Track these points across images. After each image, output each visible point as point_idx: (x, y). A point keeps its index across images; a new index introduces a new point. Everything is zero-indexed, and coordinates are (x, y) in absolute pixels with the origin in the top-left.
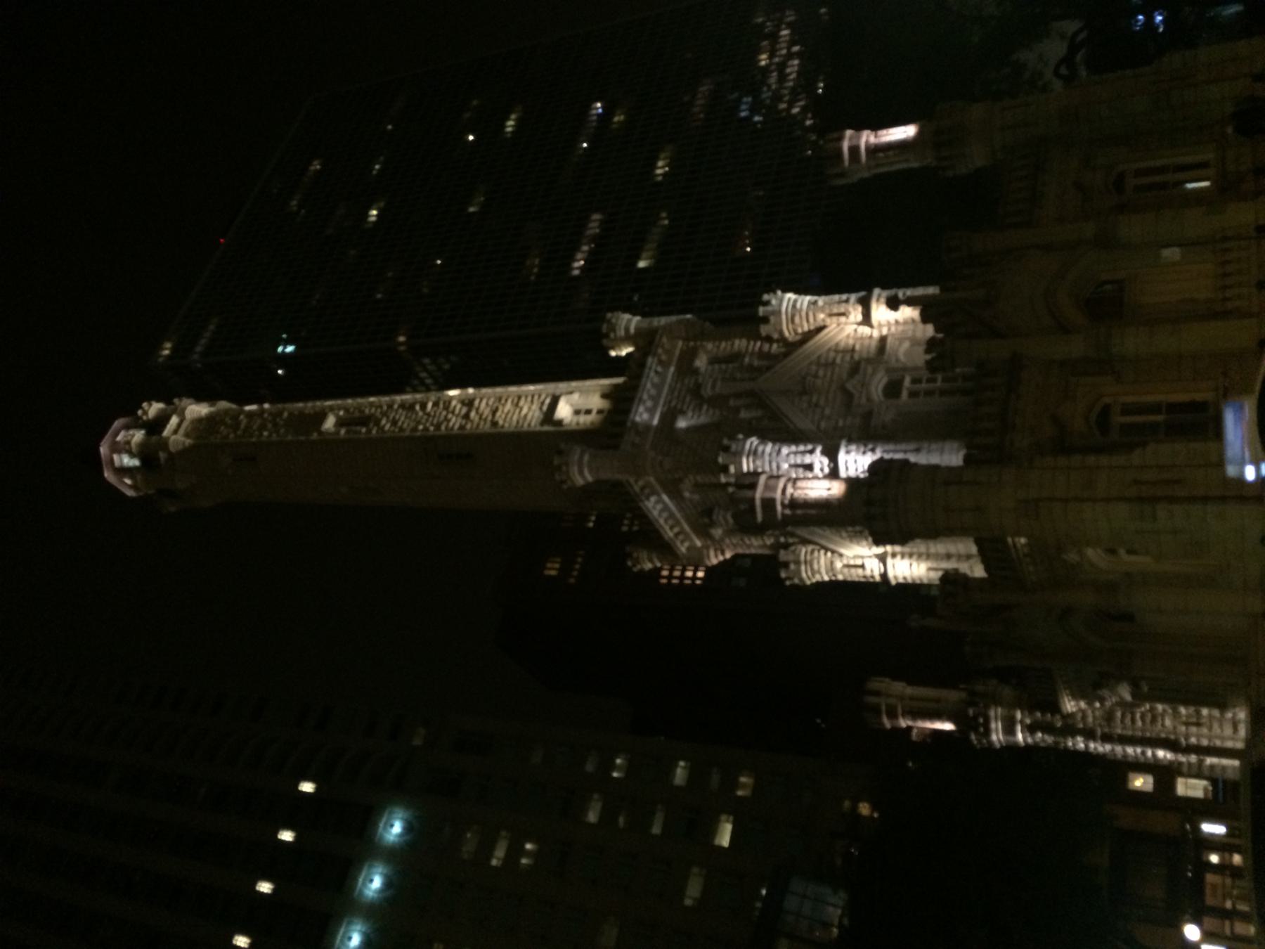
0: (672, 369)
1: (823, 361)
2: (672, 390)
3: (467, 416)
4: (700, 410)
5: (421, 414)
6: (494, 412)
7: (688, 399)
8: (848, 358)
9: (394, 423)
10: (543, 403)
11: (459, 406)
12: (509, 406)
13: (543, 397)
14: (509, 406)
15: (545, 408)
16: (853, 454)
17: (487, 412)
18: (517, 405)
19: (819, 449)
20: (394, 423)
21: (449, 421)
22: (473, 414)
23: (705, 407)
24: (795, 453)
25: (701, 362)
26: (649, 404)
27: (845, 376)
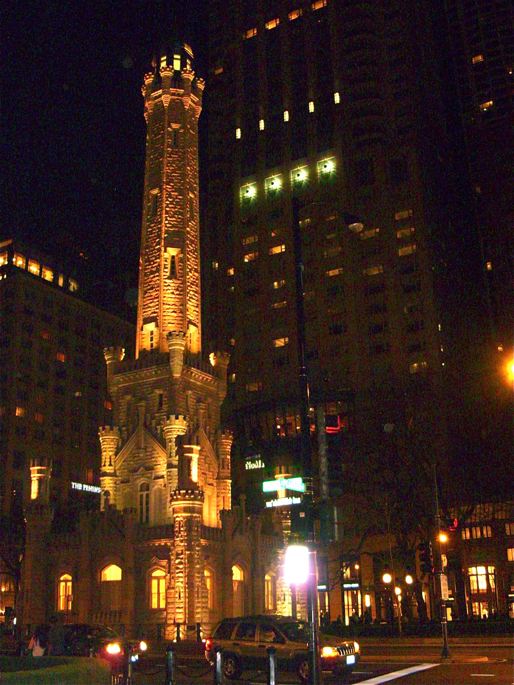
0: (155, 379)
1: (153, 452)
6: (152, 288)
8: (155, 464)
10: (155, 313)
11: (156, 265)
13: (157, 311)
22: (152, 276)
25: (158, 392)
27: (148, 465)
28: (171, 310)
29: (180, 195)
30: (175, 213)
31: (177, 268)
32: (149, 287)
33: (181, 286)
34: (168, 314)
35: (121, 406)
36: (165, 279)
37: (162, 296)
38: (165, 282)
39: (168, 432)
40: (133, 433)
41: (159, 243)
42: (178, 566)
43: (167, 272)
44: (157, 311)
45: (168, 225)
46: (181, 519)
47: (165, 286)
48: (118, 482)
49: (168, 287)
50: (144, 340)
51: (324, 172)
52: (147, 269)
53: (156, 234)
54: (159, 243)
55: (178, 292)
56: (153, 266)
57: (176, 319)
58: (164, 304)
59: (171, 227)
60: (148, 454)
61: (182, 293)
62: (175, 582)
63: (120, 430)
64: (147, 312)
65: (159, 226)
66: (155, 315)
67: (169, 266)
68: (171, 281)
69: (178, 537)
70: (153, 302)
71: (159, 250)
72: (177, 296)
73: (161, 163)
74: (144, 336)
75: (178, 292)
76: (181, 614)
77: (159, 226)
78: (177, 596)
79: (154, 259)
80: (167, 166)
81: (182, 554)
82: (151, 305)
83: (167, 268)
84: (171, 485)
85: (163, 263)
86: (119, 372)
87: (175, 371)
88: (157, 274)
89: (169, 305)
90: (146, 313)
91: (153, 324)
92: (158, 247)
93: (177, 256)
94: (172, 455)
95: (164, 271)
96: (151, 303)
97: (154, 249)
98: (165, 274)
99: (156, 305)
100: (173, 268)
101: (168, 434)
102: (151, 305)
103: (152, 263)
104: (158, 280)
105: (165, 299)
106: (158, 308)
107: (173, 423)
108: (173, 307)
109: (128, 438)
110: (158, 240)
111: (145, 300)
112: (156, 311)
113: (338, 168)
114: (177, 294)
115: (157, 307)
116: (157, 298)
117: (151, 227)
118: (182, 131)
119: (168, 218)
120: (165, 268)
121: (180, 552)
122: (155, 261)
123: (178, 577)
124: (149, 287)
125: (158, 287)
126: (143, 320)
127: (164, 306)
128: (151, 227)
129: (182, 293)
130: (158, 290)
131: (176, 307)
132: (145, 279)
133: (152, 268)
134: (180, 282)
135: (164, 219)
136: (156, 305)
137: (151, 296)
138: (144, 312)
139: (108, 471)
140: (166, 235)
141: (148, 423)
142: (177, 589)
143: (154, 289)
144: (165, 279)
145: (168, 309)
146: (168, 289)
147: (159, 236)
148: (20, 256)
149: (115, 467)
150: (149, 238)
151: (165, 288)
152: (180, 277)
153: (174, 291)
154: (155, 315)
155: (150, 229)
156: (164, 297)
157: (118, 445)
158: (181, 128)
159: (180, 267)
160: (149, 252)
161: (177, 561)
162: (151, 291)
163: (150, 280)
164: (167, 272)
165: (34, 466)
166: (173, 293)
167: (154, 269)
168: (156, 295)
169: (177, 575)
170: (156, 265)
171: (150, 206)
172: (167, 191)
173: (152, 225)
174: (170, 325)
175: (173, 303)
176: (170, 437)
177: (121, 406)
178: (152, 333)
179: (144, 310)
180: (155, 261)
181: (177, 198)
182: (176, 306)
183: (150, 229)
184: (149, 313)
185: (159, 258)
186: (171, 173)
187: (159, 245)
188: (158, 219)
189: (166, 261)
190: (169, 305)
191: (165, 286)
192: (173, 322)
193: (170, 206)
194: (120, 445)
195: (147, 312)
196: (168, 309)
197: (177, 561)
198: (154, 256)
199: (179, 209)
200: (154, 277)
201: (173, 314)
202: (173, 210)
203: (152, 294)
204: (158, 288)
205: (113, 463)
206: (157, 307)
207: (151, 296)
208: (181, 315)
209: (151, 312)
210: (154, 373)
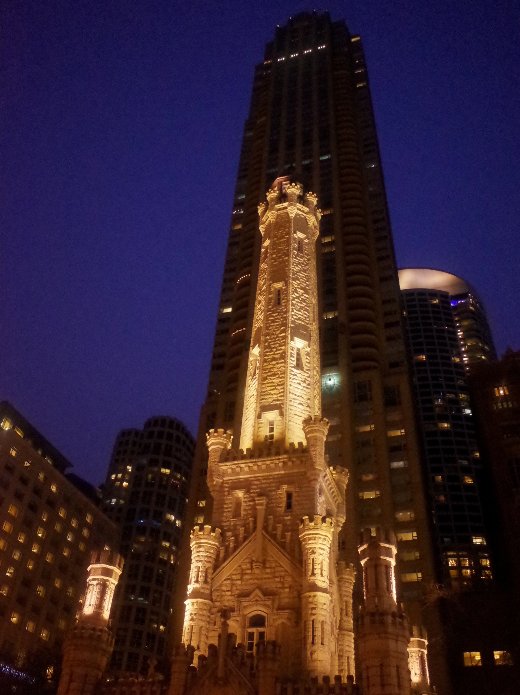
0: (283, 472)
2: (266, 478)
3: (274, 359)
4: (250, 501)
6: (274, 375)
7: (258, 490)
9: (273, 321)
10: (278, 400)
11: (280, 352)
12: (277, 381)
13: (282, 398)
14: (277, 381)
15: (274, 403)
16: (192, 608)
17: (275, 370)
18: (278, 385)
19: (198, 585)
20: (273, 321)
21: (271, 351)
22: (274, 362)
23: (251, 503)
24: (198, 572)
26: (264, 467)
28: (299, 402)
29: (305, 294)
30: (301, 308)
31: (303, 361)
32: (270, 374)
33: (309, 379)
34: (295, 405)
35: (226, 504)
36: (292, 367)
37: (289, 384)
38: (292, 371)
39: (310, 539)
40: (244, 541)
41: (284, 331)
43: (294, 361)
44: (282, 398)
45: (294, 317)
47: (292, 374)
48: (214, 610)
49: (295, 377)
50: (260, 429)
51: (329, 384)
52: (266, 356)
53: (280, 323)
54: (284, 331)
55: (305, 385)
56: (276, 353)
57: (303, 412)
58: (290, 392)
59: (298, 320)
60: (268, 571)
61: (309, 387)
63: (222, 534)
64: (266, 399)
65: (285, 315)
66: (278, 402)
67: (295, 356)
68: (298, 371)
70: (276, 389)
71: (285, 337)
72: (304, 389)
73: (288, 261)
74: (260, 425)
75: (305, 385)
77: (285, 315)
80: (293, 265)
82: (272, 392)
83: (293, 357)
84: (314, 617)
85: (290, 351)
86: (226, 460)
87: (318, 463)
88: (282, 361)
89: (296, 395)
90: (264, 401)
91: (277, 412)
92: (283, 334)
93: (303, 348)
94: (316, 572)
95: (291, 359)
96: (273, 390)
97: (278, 337)
98: (292, 362)
99: (280, 393)
100: (299, 360)
101: (310, 542)
102: (272, 392)
103: (275, 350)
104: (284, 367)
105: (291, 388)
106: (283, 396)
107: (319, 526)
108: (300, 399)
109: (235, 548)
110: (283, 328)
111: (263, 386)
112: (280, 398)
113: (342, 382)
114: (304, 387)
115: (282, 394)
116: (281, 385)
117: (273, 317)
118: (306, 241)
119: (295, 310)
120: (292, 356)
122: (279, 348)
124: (270, 374)
125: (284, 373)
126: (260, 407)
127: (291, 395)
128: (273, 317)
129: (309, 387)
130: (283, 377)
131: (303, 400)
132: (265, 365)
133: (275, 354)
134: (308, 375)
135: (291, 310)
136: (280, 393)
137: (272, 383)
138: (263, 399)
140: (292, 325)
141: (270, 529)
143: (277, 376)
144: (292, 367)
145: (294, 399)
146: (295, 379)
147: (285, 325)
148: (8, 421)
149: (211, 587)
150: (270, 326)
151: (291, 376)
152: (307, 370)
153: (301, 383)
154: (278, 402)
155: (272, 318)
156: (291, 385)
157: (218, 556)
158: (305, 238)
159: (307, 360)
160: (270, 339)
162: (272, 378)
163: (271, 366)
164: (294, 361)
165: (98, 561)
166: (299, 384)
167: (276, 356)
168: (280, 382)
170: (280, 352)
171: (272, 298)
172: (293, 286)
173: (274, 315)
174: (296, 417)
175: (300, 395)
176: (313, 546)
177: (226, 504)
178: (271, 424)
179: (262, 397)
180: (279, 348)
181: (302, 295)
182: (303, 398)
183: (272, 318)
184: (270, 400)
185: (285, 345)
186: (297, 272)
187: (285, 332)
188: (282, 309)
189: (293, 350)
190: (296, 395)
191: (292, 374)
192: (300, 414)
193: (296, 300)
194: (222, 555)
195: (266, 399)
196: (294, 399)
198: (277, 343)
199: (306, 306)
200: (278, 363)
201: (300, 406)
202: (299, 304)
203: (274, 381)
204: (283, 375)
205: (209, 580)
206: (282, 394)
207: (272, 383)
208: (308, 409)
209: (272, 399)
210: (281, 464)
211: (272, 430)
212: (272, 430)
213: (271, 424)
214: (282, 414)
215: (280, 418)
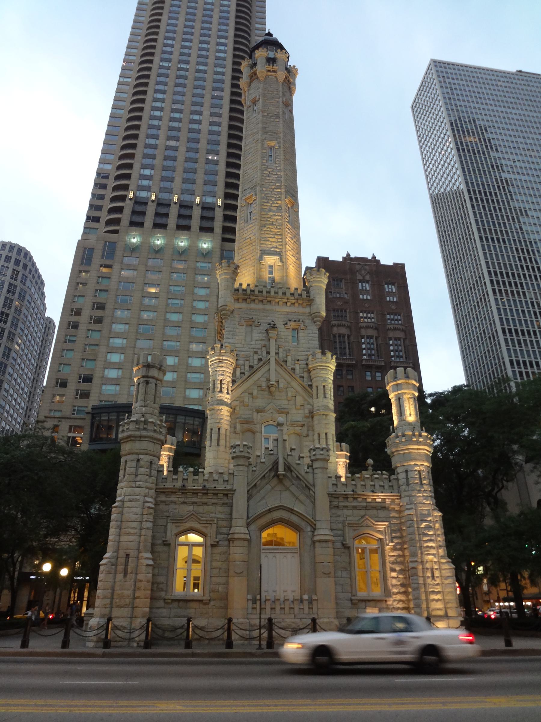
5: (273, 187)
6: (272, 224)
10: (277, 248)
11: (276, 205)
13: (281, 247)
15: (273, 249)
21: (268, 202)
22: (271, 213)
42: (426, 532)
44: (281, 247)
46: (422, 468)
62: (422, 553)
69: (419, 491)
76: (439, 603)
78: (429, 574)
79: (273, 199)
81: (429, 515)
91: (276, 258)
102: (271, 240)
121: (426, 512)
122: (275, 202)
123: (428, 547)
124: (268, 223)
139: (226, 400)
142: (428, 565)
161: (423, 525)
169: (425, 545)
170: (276, 205)
173: (269, 170)
180: (275, 202)
197: (423, 525)
200: (275, 215)
205: (230, 392)
211: (271, 273)
212: (271, 273)
213: (271, 267)
214: (281, 261)
215: (280, 264)
